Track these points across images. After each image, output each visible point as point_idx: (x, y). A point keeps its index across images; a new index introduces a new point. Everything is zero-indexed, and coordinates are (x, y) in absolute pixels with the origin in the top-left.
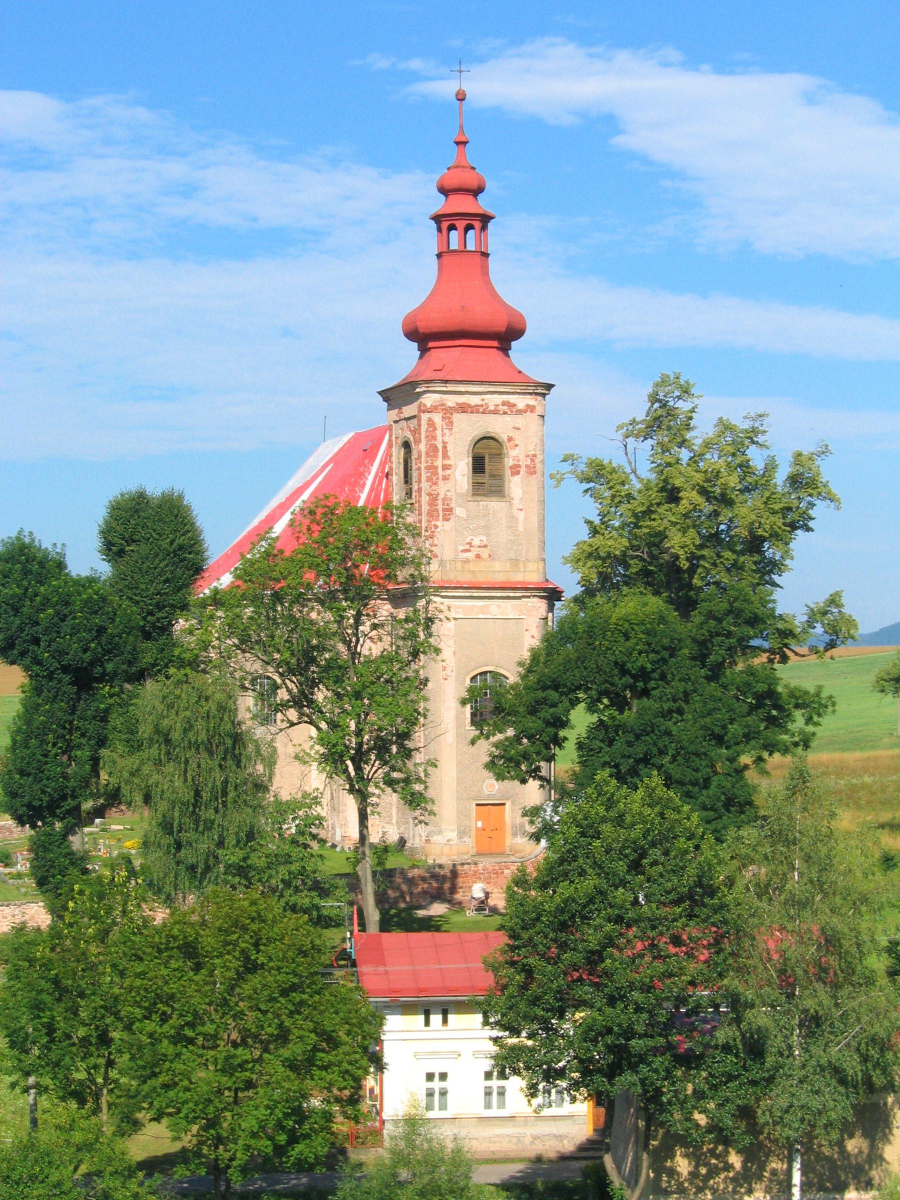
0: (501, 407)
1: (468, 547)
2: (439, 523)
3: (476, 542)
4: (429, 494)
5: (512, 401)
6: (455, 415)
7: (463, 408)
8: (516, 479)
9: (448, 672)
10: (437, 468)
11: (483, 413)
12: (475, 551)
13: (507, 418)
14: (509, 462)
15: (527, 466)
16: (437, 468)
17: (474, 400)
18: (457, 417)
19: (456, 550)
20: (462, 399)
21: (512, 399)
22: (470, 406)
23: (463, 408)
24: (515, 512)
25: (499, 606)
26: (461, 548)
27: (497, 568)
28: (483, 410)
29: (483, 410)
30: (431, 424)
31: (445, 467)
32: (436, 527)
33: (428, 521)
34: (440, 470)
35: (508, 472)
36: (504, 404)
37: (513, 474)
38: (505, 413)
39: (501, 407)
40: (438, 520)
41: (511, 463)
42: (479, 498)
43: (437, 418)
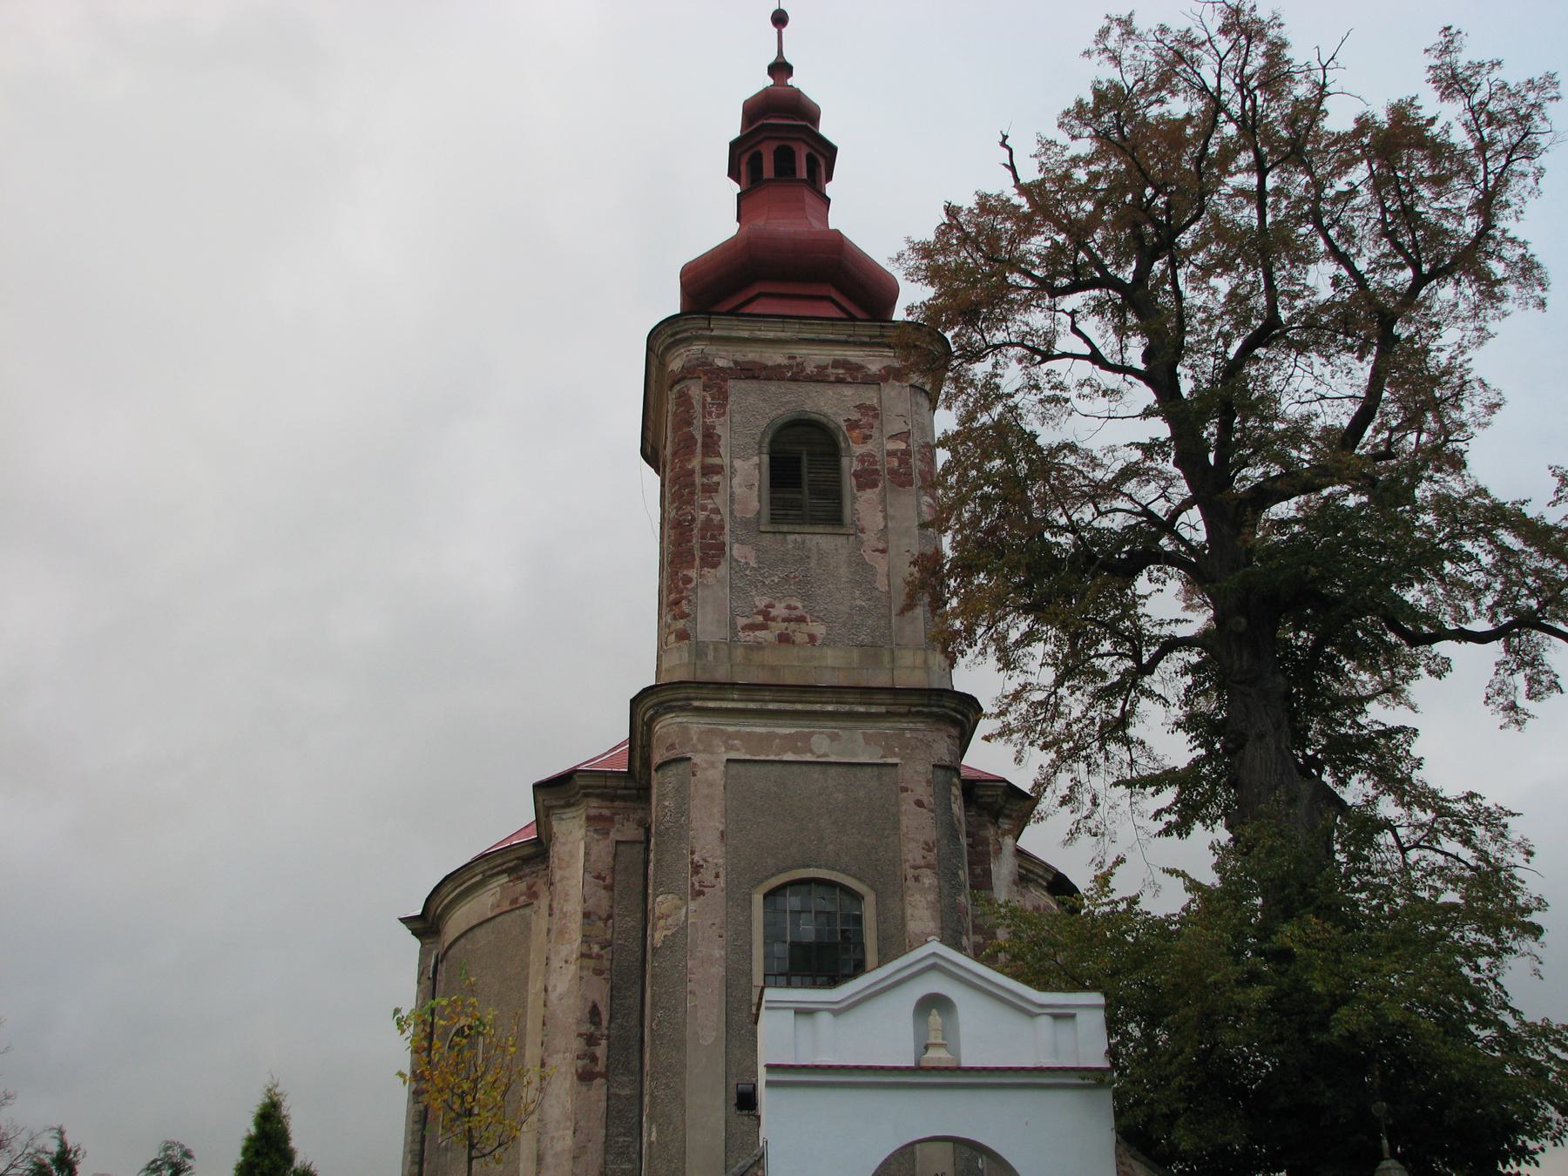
0: (830, 370)
1: (761, 618)
2: (693, 573)
3: (779, 610)
5: (853, 360)
6: (731, 383)
8: (871, 494)
9: (707, 876)
10: (693, 471)
11: (794, 379)
12: (778, 627)
13: (848, 391)
14: (850, 465)
15: (892, 472)
16: (693, 471)
18: (735, 387)
19: (733, 626)
20: (751, 354)
21: (854, 355)
22: (766, 367)
24: (868, 556)
25: (833, 738)
26: (741, 621)
27: (830, 662)
28: (797, 375)
29: (797, 375)
30: (684, 400)
31: (708, 470)
32: (688, 580)
34: (698, 479)
35: (849, 483)
36: (837, 364)
37: (861, 487)
38: (840, 381)
41: (856, 466)
42: (785, 528)
43: (695, 390)
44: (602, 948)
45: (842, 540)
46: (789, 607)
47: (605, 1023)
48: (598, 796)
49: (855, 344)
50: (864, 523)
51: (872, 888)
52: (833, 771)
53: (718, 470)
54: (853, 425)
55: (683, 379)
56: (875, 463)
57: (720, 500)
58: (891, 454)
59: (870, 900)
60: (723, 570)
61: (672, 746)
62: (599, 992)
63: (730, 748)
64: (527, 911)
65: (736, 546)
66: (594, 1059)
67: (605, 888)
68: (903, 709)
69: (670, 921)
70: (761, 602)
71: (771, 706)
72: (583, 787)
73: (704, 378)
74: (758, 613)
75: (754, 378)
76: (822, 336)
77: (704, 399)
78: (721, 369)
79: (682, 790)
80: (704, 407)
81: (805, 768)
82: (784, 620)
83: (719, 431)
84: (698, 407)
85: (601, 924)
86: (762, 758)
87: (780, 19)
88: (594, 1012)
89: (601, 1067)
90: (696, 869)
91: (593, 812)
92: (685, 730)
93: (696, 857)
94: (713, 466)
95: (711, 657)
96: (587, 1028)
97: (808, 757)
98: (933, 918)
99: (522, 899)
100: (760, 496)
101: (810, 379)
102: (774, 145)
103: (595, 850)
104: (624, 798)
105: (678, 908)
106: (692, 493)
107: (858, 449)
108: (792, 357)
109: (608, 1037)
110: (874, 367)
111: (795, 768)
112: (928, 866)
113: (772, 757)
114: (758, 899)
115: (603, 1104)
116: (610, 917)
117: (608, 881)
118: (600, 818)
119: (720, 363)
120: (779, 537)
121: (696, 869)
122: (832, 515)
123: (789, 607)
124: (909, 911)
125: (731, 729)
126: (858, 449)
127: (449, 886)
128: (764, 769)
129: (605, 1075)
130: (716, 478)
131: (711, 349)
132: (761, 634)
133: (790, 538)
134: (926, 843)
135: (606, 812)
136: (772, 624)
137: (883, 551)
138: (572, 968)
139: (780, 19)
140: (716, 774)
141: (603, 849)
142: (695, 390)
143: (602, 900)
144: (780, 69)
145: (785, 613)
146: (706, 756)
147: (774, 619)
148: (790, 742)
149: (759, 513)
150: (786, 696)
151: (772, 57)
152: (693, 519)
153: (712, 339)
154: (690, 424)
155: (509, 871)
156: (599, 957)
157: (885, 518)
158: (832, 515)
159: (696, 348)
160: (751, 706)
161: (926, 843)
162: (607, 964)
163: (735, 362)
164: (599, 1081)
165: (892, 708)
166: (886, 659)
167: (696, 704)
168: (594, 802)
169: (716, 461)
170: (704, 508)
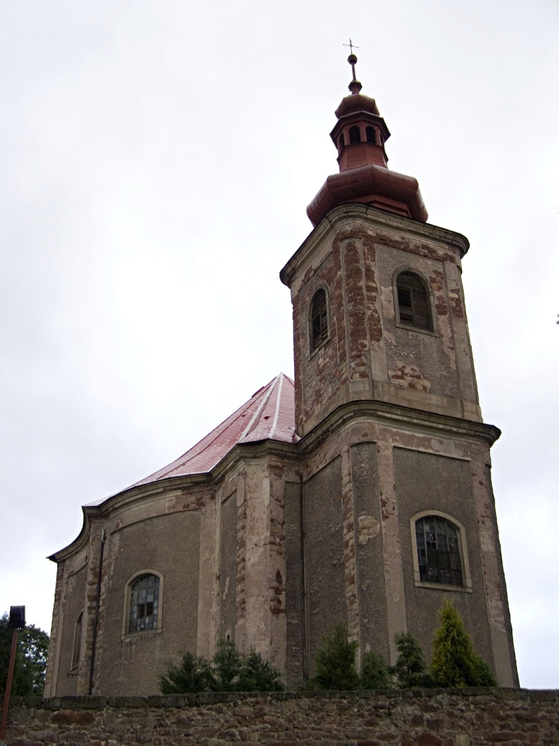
0: (421, 250)
1: (400, 373)
2: (366, 342)
3: (408, 370)
4: (351, 315)
5: (431, 246)
7: (384, 241)
8: (442, 318)
11: (404, 250)
13: (430, 262)
14: (434, 301)
16: (361, 288)
17: (396, 236)
19: (388, 376)
23: (384, 241)
24: (446, 350)
25: (441, 442)
26: (391, 373)
27: (434, 402)
30: (351, 248)
32: (365, 346)
33: (352, 341)
35: (434, 310)
36: (424, 247)
38: (425, 256)
39: (421, 250)
40: (366, 339)
41: (436, 302)
42: (408, 328)
44: (281, 540)
45: (433, 339)
46: (412, 369)
47: (284, 582)
48: (276, 455)
49: (432, 238)
50: (443, 332)
51: (464, 524)
52: (441, 460)
53: (375, 290)
54: (433, 281)
55: (351, 237)
56: (444, 302)
57: (377, 306)
58: (452, 299)
59: (463, 530)
60: (382, 343)
61: (366, 435)
62: (280, 564)
63: (394, 440)
64: (196, 513)
65: (386, 332)
66: (279, 602)
67: (281, 506)
68: (472, 433)
69: (371, 531)
70: (400, 364)
71: (415, 421)
72: (270, 449)
73: (363, 239)
74: (399, 370)
75: (386, 245)
76: (418, 231)
77: (364, 250)
78: (371, 236)
79: (372, 458)
80: (364, 255)
81: (428, 456)
82: (411, 376)
83: (373, 268)
84: (361, 253)
85: (279, 526)
86: (410, 448)
87: (353, 60)
88: (278, 575)
89: (283, 607)
90: (384, 503)
91: (273, 463)
92: (372, 426)
93: (384, 497)
94: (372, 287)
95: (380, 389)
96: (275, 584)
97: (430, 451)
98: (492, 544)
99: (193, 506)
100: (394, 307)
101: (412, 252)
102: (367, 125)
103: (275, 484)
104: (289, 458)
105: (375, 524)
106: (362, 299)
107: (437, 293)
108: (403, 238)
109: (286, 590)
110: (441, 253)
111: (424, 456)
112: (487, 517)
113: (414, 448)
114: (413, 524)
115: (285, 628)
116: (284, 523)
117: (282, 503)
118: (276, 467)
119: (370, 233)
120: (406, 331)
121: (384, 503)
122: (428, 326)
123: (412, 369)
124: (481, 539)
125: (394, 430)
126: (437, 293)
127: (134, 493)
128: (410, 454)
129: (284, 611)
130: (374, 294)
131: (366, 224)
132: (401, 381)
133: (410, 333)
134: (486, 504)
135: (280, 465)
136: (406, 377)
137: (452, 349)
138: (261, 549)
139: (353, 60)
140: (389, 453)
141: (279, 484)
142: (359, 244)
143: (279, 514)
144: (355, 86)
145: (411, 372)
146: (384, 443)
147: (406, 375)
148: (422, 441)
149: (395, 316)
150: (423, 416)
151: (351, 79)
152: (364, 314)
153: (366, 219)
154: (357, 262)
155: (183, 489)
156: (280, 545)
157: (452, 331)
158: (428, 326)
159: (359, 222)
160: (406, 419)
161: (486, 504)
162: (284, 549)
163: (377, 234)
164: (282, 615)
165: (468, 432)
166: (459, 405)
167: (380, 413)
168: (274, 458)
169: (373, 284)
170: (369, 308)
